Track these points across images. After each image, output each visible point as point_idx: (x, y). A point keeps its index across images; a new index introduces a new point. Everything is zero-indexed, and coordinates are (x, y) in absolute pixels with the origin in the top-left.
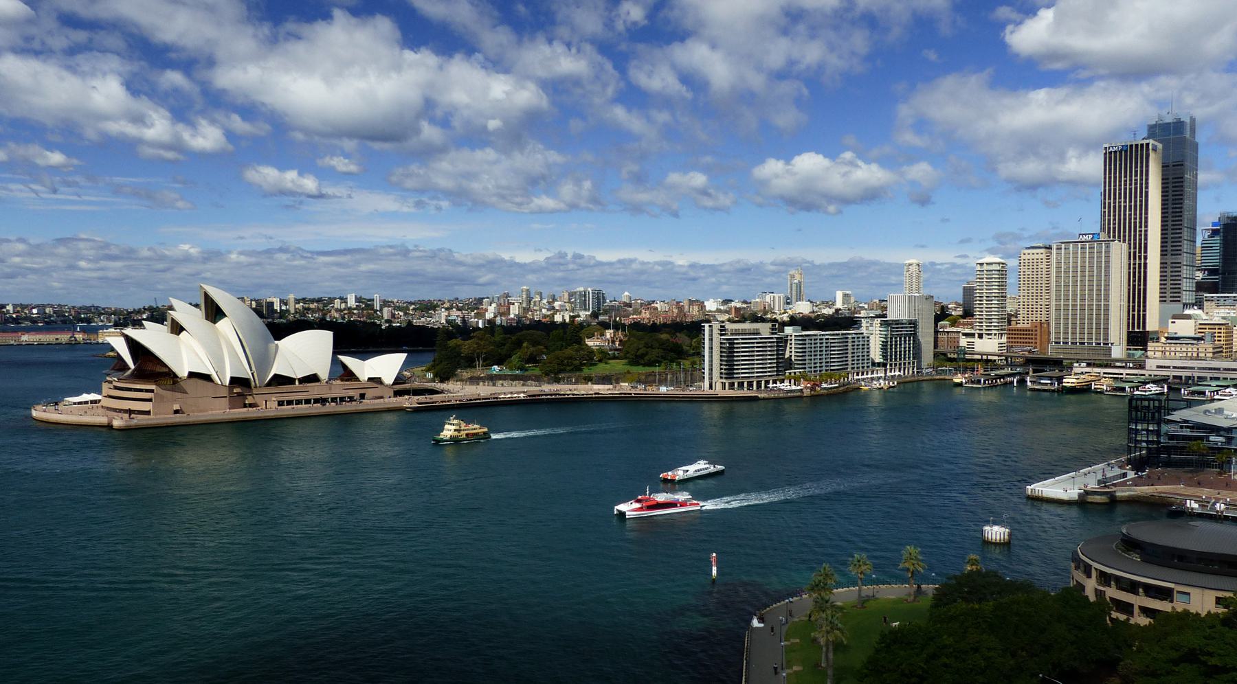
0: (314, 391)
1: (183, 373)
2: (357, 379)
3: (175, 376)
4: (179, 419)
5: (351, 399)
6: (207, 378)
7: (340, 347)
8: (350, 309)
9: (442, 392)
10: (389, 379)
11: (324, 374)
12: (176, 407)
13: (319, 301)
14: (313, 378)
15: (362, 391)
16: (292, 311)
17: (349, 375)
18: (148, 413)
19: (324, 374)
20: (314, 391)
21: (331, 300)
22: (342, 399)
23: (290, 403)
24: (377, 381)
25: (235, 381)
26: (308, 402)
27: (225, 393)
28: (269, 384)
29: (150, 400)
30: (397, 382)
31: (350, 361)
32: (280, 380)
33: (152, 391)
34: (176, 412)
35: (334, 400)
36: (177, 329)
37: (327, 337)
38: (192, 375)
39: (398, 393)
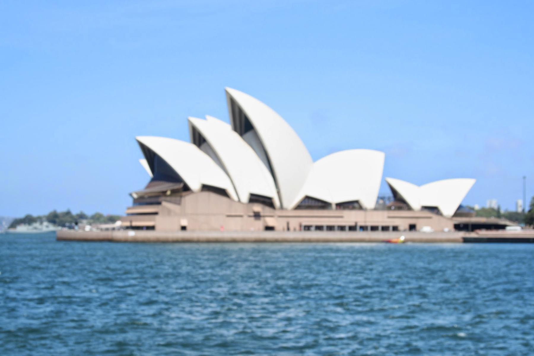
0: (350, 217)
1: (194, 185)
2: (409, 208)
3: (186, 188)
5: (395, 229)
6: (222, 192)
10: (448, 209)
12: (184, 223)
15: (412, 222)
19: (369, 201)
20: (350, 217)
22: (385, 229)
23: (319, 228)
24: (434, 209)
25: (255, 199)
26: (342, 228)
28: (299, 207)
29: (156, 213)
30: (460, 212)
32: (311, 203)
34: (184, 228)
35: (374, 228)
38: (206, 188)
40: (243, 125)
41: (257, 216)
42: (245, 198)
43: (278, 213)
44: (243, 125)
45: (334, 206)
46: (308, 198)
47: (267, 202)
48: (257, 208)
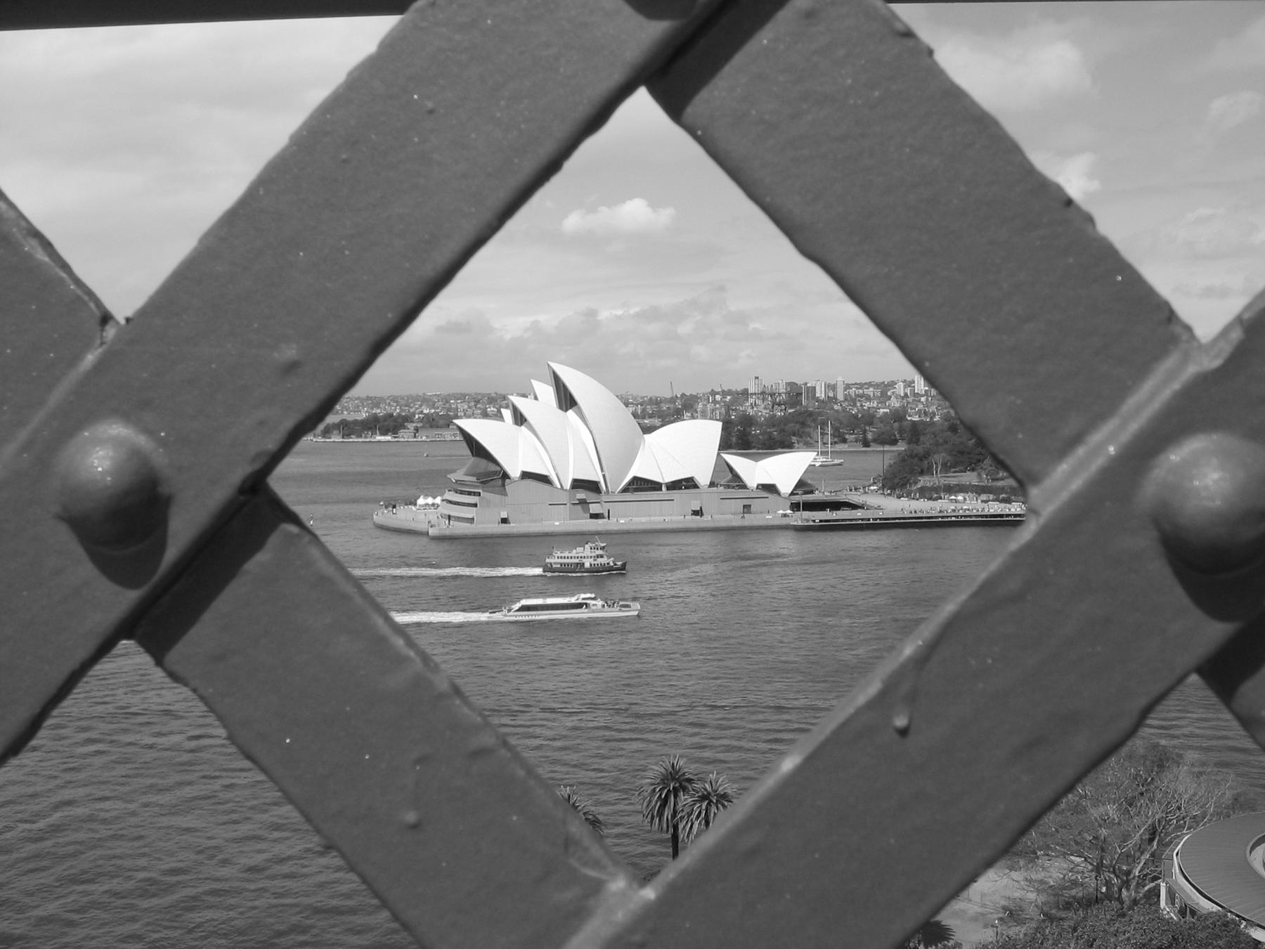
1: (515, 473)
2: (744, 487)
3: (505, 476)
4: (504, 528)
6: (545, 479)
7: (725, 445)
8: (916, 395)
9: (862, 507)
10: (786, 487)
11: (703, 479)
12: (504, 515)
13: (877, 386)
14: (688, 484)
15: (747, 502)
16: (840, 397)
17: (736, 481)
18: (471, 520)
19: (703, 479)
21: (892, 384)
24: (770, 489)
25: (578, 484)
27: (564, 498)
28: (625, 490)
29: (475, 505)
31: (738, 462)
33: (479, 494)
34: (504, 521)
36: (520, 419)
37: (714, 429)
38: (526, 475)
39: (795, 507)
40: (566, 400)
41: (583, 502)
42: (568, 485)
43: (604, 498)
44: (566, 400)
45: (664, 488)
46: (636, 480)
47: (593, 486)
48: (581, 495)
